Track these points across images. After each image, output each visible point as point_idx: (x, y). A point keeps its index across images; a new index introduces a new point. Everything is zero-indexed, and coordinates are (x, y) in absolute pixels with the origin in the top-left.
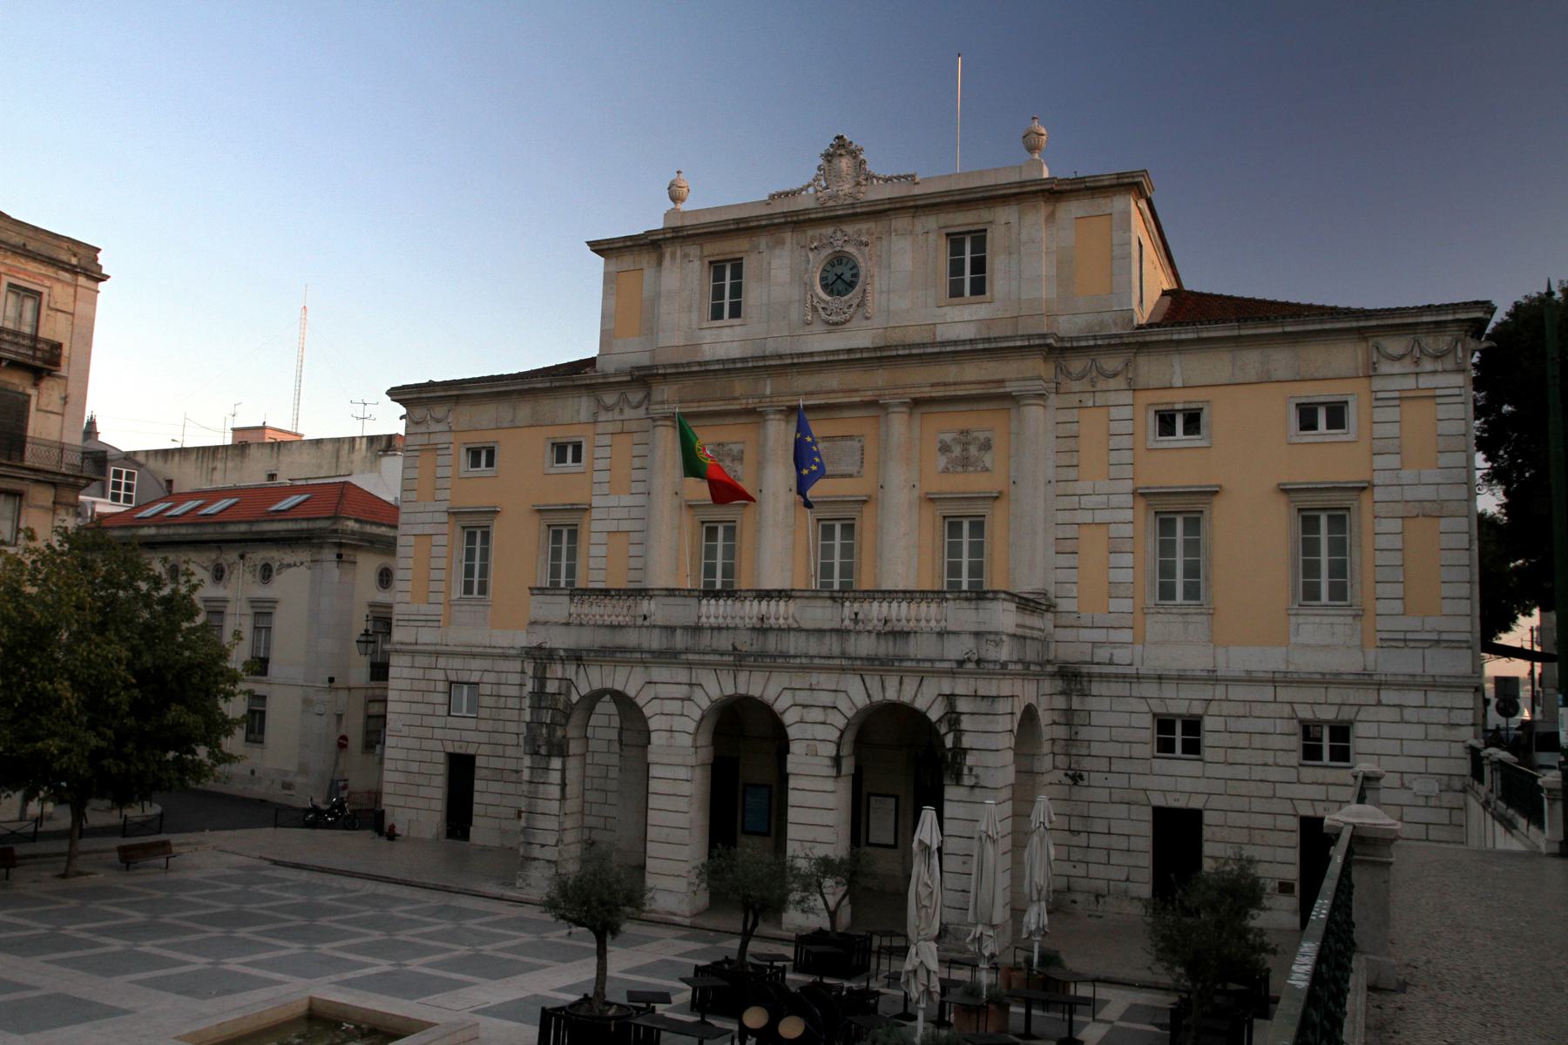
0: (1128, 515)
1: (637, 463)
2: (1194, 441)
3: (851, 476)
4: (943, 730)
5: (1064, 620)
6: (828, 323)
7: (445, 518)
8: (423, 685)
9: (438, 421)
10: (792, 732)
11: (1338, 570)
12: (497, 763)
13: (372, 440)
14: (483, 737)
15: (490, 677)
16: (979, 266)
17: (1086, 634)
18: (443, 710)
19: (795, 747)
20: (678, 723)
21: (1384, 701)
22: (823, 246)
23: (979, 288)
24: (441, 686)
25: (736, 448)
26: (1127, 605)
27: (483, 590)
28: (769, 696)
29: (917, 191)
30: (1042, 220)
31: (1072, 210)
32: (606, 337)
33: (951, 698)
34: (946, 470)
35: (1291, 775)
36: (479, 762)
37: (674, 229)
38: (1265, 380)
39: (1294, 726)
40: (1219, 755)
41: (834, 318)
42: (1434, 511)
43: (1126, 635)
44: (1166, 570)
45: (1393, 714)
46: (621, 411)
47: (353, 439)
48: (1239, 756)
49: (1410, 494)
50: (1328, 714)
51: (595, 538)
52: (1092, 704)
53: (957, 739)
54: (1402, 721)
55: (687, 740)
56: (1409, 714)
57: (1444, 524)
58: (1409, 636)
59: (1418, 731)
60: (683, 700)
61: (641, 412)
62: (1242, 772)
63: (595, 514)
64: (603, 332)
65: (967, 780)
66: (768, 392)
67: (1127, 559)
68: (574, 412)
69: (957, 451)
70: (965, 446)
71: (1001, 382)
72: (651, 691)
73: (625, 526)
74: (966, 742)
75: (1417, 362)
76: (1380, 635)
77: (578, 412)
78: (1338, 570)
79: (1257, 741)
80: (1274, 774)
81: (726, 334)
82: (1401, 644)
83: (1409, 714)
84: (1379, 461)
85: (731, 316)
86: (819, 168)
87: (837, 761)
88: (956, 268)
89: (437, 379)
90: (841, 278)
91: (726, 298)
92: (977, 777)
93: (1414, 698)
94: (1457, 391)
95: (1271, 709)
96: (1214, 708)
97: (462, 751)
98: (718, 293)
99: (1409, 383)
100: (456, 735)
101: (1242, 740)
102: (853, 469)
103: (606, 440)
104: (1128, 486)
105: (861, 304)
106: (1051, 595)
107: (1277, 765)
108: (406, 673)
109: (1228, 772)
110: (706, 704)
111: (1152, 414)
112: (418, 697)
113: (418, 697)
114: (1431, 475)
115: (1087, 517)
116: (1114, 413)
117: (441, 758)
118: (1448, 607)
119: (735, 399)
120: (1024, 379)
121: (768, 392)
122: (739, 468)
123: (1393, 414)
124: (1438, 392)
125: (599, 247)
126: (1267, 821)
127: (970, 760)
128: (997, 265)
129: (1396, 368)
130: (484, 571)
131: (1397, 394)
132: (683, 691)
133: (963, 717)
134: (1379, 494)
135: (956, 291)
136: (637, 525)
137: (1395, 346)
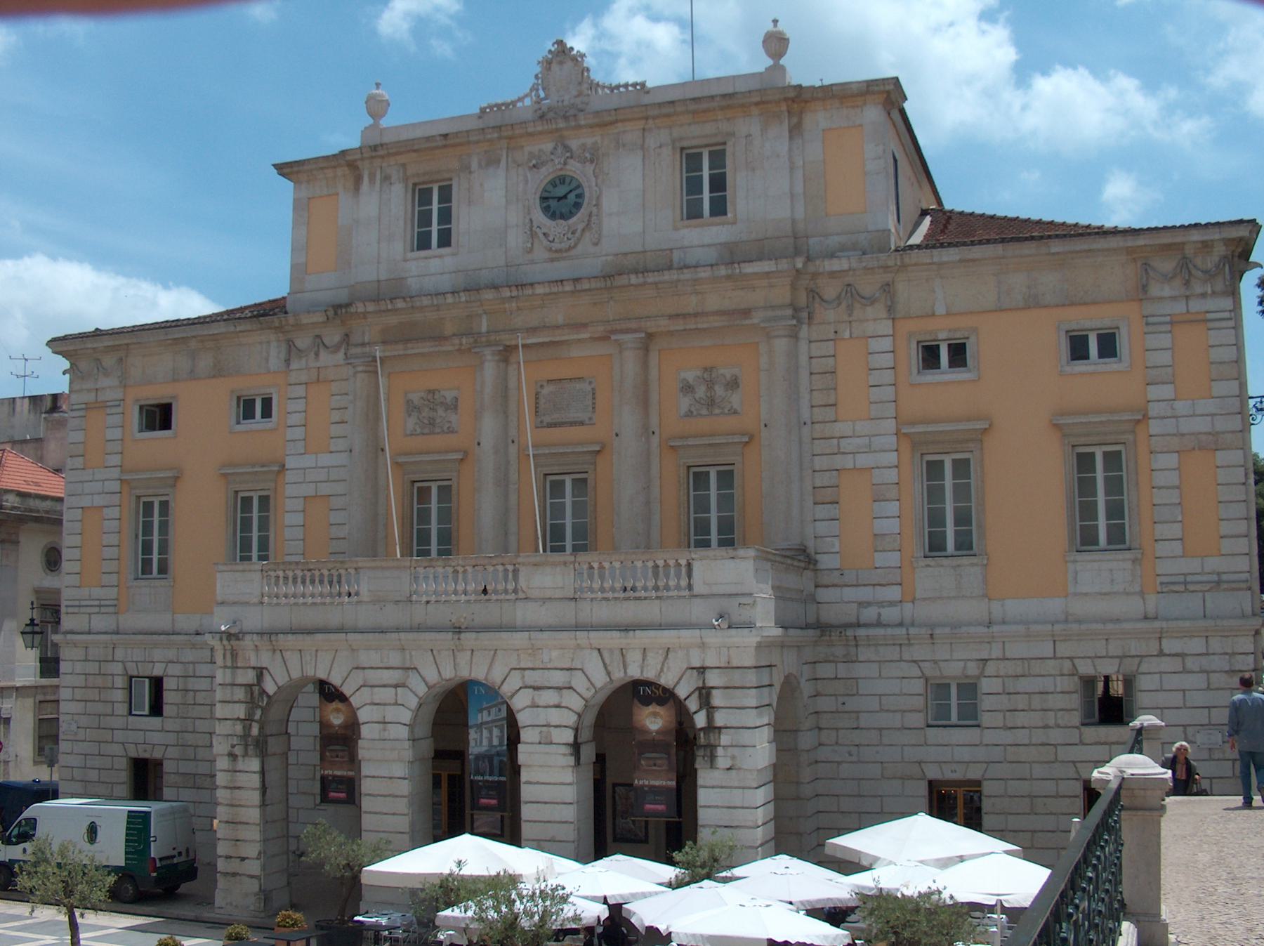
0: (892, 458)
2: (959, 375)
3: (582, 423)
4: (692, 705)
5: (825, 580)
6: (550, 250)
7: (116, 486)
8: (99, 681)
9: (107, 374)
11: (1116, 511)
12: (186, 767)
13: (35, 400)
14: (171, 739)
15: (175, 670)
16: (718, 183)
17: (849, 594)
18: (122, 709)
20: (391, 713)
21: (1166, 651)
22: (543, 163)
23: (719, 208)
24: (120, 682)
25: (449, 395)
26: (893, 559)
27: (163, 569)
28: (496, 676)
29: (647, 100)
30: (786, 134)
32: (298, 272)
33: (702, 670)
34: (689, 414)
35: (1074, 736)
36: (168, 767)
37: (375, 148)
38: (1033, 303)
39: (1074, 683)
40: (998, 720)
41: (556, 246)
42: (1212, 443)
43: (894, 593)
44: (936, 519)
45: (1175, 664)
46: (317, 354)
47: (13, 400)
48: (1021, 718)
49: (1186, 426)
51: (290, 504)
52: (860, 670)
53: (710, 718)
54: (1185, 671)
55: (404, 732)
56: (1190, 663)
57: (1222, 457)
58: (1189, 579)
59: (1198, 681)
60: (396, 686)
61: (340, 356)
62: (1021, 736)
63: (290, 476)
64: (294, 267)
65: (722, 762)
67: (893, 508)
68: (261, 361)
69: (701, 392)
70: (710, 384)
72: (358, 678)
73: (325, 489)
74: (720, 720)
75: (1187, 283)
77: (267, 360)
78: (1116, 511)
79: (1037, 702)
80: (1055, 736)
81: (435, 265)
82: (1181, 588)
83: (1190, 663)
84: (1154, 392)
85: (439, 246)
86: (536, 77)
87: (576, 747)
88: (693, 186)
89: (104, 326)
90: (561, 200)
91: (432, 222)
92: (733, 758)
93: (1196, 645)
94: (1226, 315)
95: (1051, 666)
96: (991, 669)
97: (147, 756)
98: (425, 219)
99: (1180, 308)
100: (139, 737)
101: (1021, 702)
103: (300, 391)
104: (890, 425)
105: (588, 226)
106: (811, 550)
107: (1058, 726)
108: (79, 667)
109: (1008, 737)
110: (422, 690)
111: (914, 345)
112: (93, 695)
113: (93, 695)
115: (848, 462)
116: (875, 345)
117: (123, 764)
118: (1226, 546)
119: (446, 338)
120: (773, 307)
121: (484, 329)
122: (453, 418)
123: (1165, 340)
125: (285, 169)
126: (1049, 787)
127: (725, 739)
128: (738, 181)
129: (1167, 291)
130: (164, 549)
133: (714, 692)
134: (1155, 427)
136: (340, 488)
137: (1166, 265)
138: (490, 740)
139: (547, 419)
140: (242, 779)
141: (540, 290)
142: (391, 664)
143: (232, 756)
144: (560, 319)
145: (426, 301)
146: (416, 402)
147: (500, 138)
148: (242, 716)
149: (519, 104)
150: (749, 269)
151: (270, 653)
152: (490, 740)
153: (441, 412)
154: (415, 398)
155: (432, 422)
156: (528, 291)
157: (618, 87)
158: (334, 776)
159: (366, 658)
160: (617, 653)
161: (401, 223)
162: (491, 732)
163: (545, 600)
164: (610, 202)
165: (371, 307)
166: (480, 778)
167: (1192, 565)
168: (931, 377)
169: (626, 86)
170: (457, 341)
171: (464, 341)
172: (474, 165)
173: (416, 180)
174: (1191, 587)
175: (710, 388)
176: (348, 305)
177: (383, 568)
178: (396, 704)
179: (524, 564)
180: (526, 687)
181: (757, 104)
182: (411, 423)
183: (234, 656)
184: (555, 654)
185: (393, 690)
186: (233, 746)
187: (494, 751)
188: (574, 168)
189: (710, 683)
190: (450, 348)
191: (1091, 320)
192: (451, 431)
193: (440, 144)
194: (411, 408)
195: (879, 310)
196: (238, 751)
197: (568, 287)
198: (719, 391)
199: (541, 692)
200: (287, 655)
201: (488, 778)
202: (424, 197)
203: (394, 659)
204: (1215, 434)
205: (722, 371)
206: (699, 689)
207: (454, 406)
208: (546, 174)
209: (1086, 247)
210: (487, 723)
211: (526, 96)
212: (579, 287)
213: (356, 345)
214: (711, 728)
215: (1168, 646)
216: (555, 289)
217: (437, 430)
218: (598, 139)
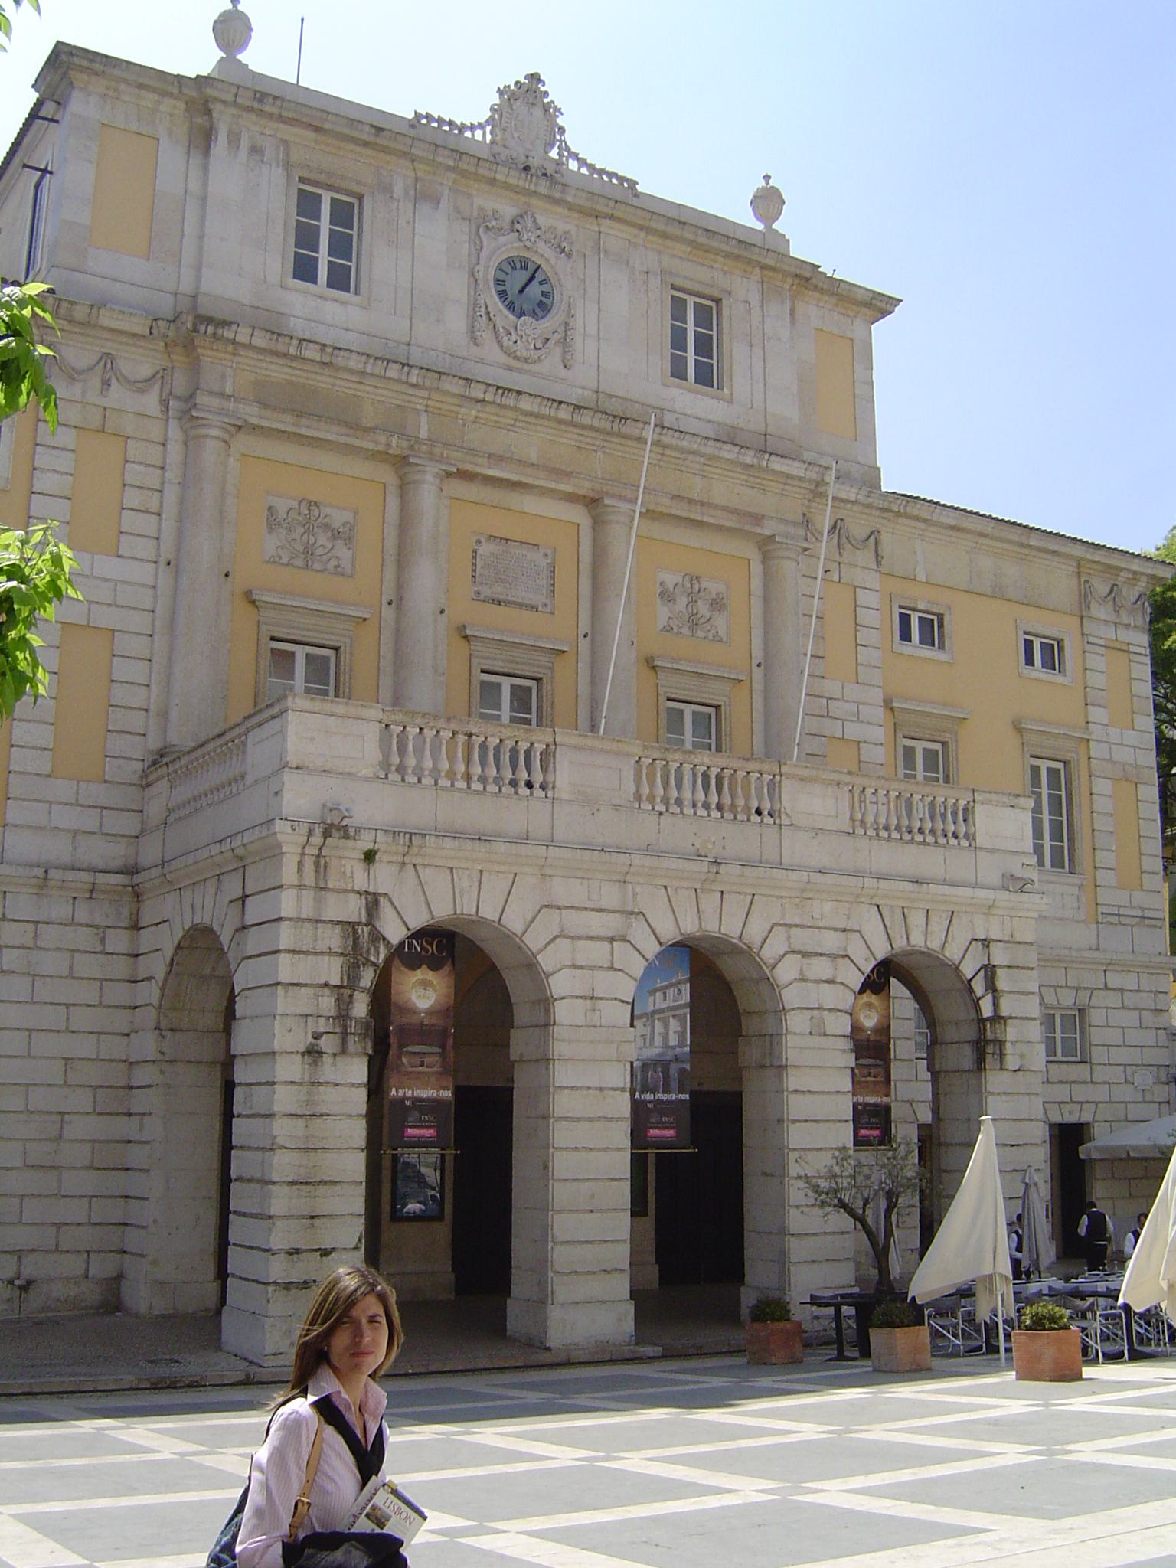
1: (133, 498)
2: (927, 652)
10: (791, 997)
16: (704, 346)
19: (797, 1023)
25: (339, 518)
28: (755, 933)
29: (635, 202)
31: (814, 312)
33: (986, 943)
34: (667, 629)
38: (997, 593)
41: (521, 350)
46: (106, 384)
50: (1068, 999)
53: (996, 1005)
60: (611, 940)
65: (1011, 1062)
66: (423, 434)
69: (682, 601)
71: (758, 519)
72: (550, 923)
73: (105, 618)
76: (1100, 909)
84: (1097, 714)
85: (330, 285)
86: (492, 109)
90: (525, 291)
92: (1022, 1056)
93: (1130, 982)
98: (306, 237)
102: (539, 600)
103: (66, 438)
104: (877, 695)
110: (652, 949)
114: (1131, 737)
119: (367, 430)
120: (787, 522)
122: (342, 551)
124: (1132, 649)
131: (1102, 642)
132: (609, 924)
133: (999, 971)
135: (678, 371)
138: (665, 1037)
139: (486, 591)
140: (329, 1099)
141: (525, 404)
142: (603, 904)
143: (313, 1053)
144: (533, 455)
145: (355, 362)
146: (282, 515)
147: (449, 168)
148: (335, 980)
149: (468, 134)
150: (777, 464)
151: (394, 869)
152: (665, 1037)
153: (323, 539)
154: (282, 505)
155: (308, 552)
156: (510, 401)
157: (602, 172)
158: (416, 1100)
159: (565, 891)
160: (899, 912)
161: (279, 229)
162: (666, 1027)
163: (818, 831)
164: (584, 319)
165: (260, 340)
166: (649, 1097)
167: (1121, 897)
168: (905, 648)
169: (611, 175)
170: (382, 439)
171: (394, 441)
172: (398, 191)
173: (305, 174)
174: (1124, 920)
175: (692, 602)
176: (225, 323)
177: (592, 749)
178: (612, 968)
179: (789, 776)
180: (794, 952)
181: (763, 267)
182: (272, 543)
183: (321, 866)
184: (828, 906)
185: (606, 945)
186: (317, 1036)
187: (669, 1056)
188: (544, 255)
189: (996, 960)
190: (370, 446)
191: (1048, 625)
192: (338, 571)
193: (365, 137)
194: (273, 520)
195: (866, 557)
196: (327, 1044)
197: (564, 414)
198: (703, 609)
199: (814, 961)
200: (426, 874)
201: (660, 1096)
202: (308, 204)
203: (610, 896)
204: (1137, 767)
205: (704, 585)
206: (984, 967)
207: (343, 535)
208: (507, 246)
209: (1056, 548)
210: (662, 1011)
211: (481, 126)
212: (577, 418)
213: (211, 393)
214: (997, 1018)
215: (1114, 980)
216: (545, 411)
217: (317, 566)
218: (573, 230)
